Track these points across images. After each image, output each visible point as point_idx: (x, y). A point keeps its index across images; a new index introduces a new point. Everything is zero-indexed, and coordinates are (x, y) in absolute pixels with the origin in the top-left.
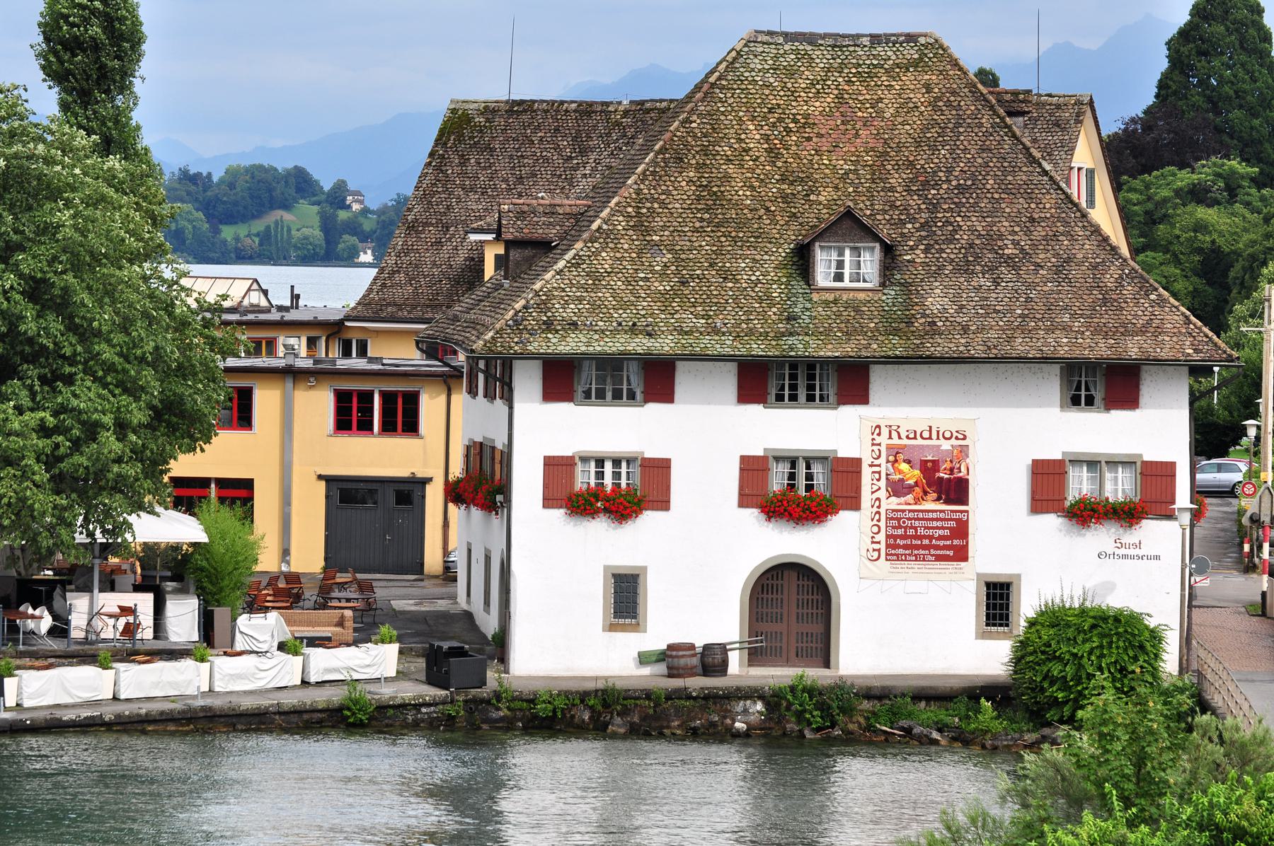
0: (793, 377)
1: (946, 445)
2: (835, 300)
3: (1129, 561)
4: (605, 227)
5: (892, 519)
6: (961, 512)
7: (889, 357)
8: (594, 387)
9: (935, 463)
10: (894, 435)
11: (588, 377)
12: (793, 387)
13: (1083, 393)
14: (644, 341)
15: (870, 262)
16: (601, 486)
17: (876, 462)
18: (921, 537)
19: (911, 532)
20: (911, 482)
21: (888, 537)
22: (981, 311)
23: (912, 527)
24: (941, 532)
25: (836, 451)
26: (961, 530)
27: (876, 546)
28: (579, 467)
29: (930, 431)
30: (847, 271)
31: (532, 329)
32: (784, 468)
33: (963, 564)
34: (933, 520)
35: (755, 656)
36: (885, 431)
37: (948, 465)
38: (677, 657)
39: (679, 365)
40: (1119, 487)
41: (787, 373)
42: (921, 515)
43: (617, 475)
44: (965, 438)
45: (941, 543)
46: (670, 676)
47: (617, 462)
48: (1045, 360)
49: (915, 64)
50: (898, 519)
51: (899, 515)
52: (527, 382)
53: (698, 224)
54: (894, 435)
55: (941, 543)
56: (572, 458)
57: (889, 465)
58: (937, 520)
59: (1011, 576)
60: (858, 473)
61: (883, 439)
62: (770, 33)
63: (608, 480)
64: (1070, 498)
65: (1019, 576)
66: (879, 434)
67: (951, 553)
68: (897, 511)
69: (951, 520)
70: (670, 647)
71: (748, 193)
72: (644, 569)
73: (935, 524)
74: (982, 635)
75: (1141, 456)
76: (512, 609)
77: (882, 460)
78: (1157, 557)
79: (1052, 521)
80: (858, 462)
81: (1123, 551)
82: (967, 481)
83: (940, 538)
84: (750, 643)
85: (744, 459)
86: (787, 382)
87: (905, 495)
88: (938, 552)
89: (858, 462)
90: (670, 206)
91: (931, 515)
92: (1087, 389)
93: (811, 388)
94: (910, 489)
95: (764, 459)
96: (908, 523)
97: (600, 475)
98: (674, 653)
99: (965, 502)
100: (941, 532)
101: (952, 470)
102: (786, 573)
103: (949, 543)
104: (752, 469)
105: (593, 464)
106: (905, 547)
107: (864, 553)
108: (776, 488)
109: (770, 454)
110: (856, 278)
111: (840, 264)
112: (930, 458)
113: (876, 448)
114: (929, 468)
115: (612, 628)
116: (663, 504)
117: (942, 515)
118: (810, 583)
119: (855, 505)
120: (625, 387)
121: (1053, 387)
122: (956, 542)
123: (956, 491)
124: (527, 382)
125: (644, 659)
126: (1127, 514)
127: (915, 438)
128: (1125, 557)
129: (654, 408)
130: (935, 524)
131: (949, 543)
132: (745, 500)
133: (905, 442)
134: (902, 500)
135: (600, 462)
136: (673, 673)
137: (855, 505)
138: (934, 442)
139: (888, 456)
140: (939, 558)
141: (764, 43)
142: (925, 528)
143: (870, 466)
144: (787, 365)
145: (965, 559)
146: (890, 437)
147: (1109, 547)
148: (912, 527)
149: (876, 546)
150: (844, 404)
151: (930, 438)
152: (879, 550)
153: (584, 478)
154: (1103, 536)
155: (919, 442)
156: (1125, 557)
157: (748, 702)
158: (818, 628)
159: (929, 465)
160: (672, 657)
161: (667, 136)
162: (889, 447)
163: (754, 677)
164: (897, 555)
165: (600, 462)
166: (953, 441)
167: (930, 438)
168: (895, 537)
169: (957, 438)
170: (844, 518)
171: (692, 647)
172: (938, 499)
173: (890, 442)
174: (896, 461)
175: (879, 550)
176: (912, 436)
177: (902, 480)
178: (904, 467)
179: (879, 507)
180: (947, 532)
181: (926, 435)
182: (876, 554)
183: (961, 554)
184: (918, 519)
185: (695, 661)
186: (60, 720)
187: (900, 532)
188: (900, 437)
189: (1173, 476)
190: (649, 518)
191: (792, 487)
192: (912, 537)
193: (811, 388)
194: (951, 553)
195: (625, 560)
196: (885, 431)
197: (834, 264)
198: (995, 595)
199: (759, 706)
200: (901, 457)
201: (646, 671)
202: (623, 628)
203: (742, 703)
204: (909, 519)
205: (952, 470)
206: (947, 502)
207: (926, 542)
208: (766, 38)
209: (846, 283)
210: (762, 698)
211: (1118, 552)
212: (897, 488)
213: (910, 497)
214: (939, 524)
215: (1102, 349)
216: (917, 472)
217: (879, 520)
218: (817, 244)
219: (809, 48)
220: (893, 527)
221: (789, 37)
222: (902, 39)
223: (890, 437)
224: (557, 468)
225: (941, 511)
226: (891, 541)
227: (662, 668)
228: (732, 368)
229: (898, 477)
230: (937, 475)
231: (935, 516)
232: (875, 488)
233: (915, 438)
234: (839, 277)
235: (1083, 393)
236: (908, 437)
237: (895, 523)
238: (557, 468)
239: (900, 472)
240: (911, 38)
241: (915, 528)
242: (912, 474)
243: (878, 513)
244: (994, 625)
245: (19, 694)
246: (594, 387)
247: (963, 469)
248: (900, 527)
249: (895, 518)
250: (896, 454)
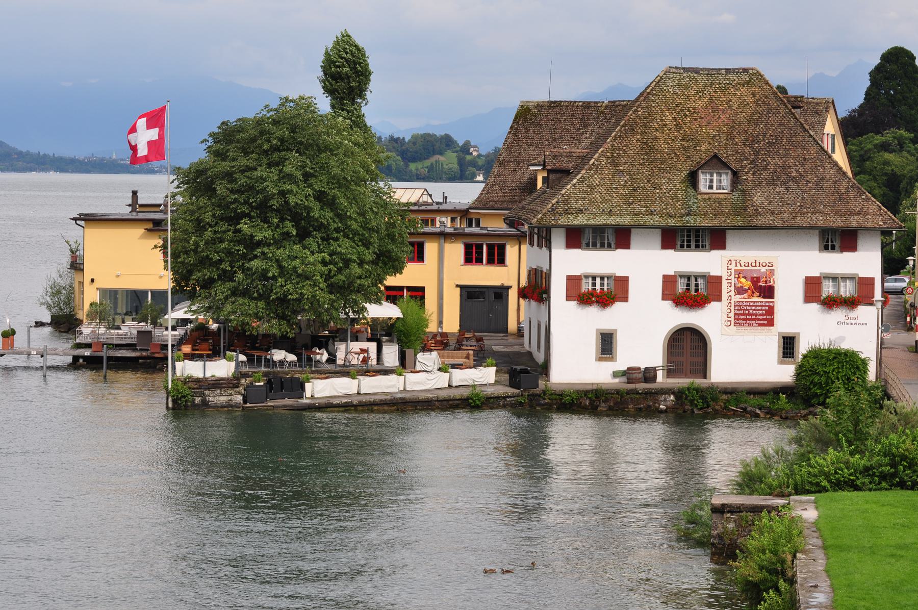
0: (688, 236)
1: (763, 270)
2: (709, 198)
4: (596, 163)
5: (737, 306)
6: (771, 302)
7: (735, 226)
8: (591, 241)
9: (758, 278)
10: (738, 264)
11: (588, 236)
12: (689, 241)
13: (830, 244)
15: (726, 180)
16: (594, 289)
17: (729, 278)
18: (751, 315)
19: (746, 312)
20: (747, 288)
21: (735, 314)
22: (780, 204)
23: (746, 310)
24: (761, 312)
25: (709, 273)
26: (771, 311)
27: (729, 319)
28: (584, 280)
29: (756, 262)
30: (715, 184)
31: (561, 213)
32: (685, 281)
33: (771, 328)
34: (757, 306)
35: (670, 373)
36: (733, 263)
37: (764, 279)
38: (632, 373)
39: (633, 230)
40: (847, 290)
42: (751, 304)
43: (602, 285)
44: (772, 266)
45: (761, 317)
46: (628, 383)
47: (602, 278)
48: (811, 228)
49: (748, 83)
50: (740, 306)
51: (740, 304)
52: (559, 239)
53: (641, 161)
54: (738, 264)
55: (761, 317)
56: (580, 276)
57: (736, 279)
58: (759, 306)
59: (795, 333)
60: (721, 283)
61: (733, 267)
62: (677, 68)
63: (598, 287)
64: (824, 295)
65: (799, 333)
66: (731, 264)
67: (766, 322)
68: (740, 302)
69: (766, 306)
70: (629, 369)
71: (666, 146)
72: (616, 330)
73: (758, 308)
74: (781, 362)
75: (858, 274)
76: (551, 350)
77: (732, 277)
78: (865, 324)
79: (815, 307)
80: (720, 278)
82: (774, 287)
83: (761, 315)
84: (667, 366)
85: (664, 276)
86: (685, 239)
87: (743, 294)
88: (761, 322)
89: (720, 278)
90: (628, 153)
91: (756, 304)
92: (832, 242)
93: (697, 241)
94: (746, 291)
95: (674, 276)
96: (745, 308)
97: (594, 284)
98: (630, 372)
99: (773, 297)
100: (761, 312)
101: (766, 282)
103: (765, 317)
104: (669, 282)
105: (590, 279)
106: (743, 319)
107: (723, 322)
108: (680, 291)
109: (677, 274)
110: (719, 187)
111: (711, 181)
112: (755, 276)
113: (729, 271)
114: (755, 281)
115: (600, 359)
116: (625, 299)
117: (761, 304)
118: (697, 337)
119: (719, 299)
120: (606, 241)
121: (815, 241)
122: (768, 317)
123: (768, 292)
124: (559, 239)
125: (615, 374)
126: (851, 303)
127: (748, 266)
128: (850, 324)
129: (621, 252)
130: (758, 308)
131: (765, 317)
132: (665, 297)
133: (743, 268)
134: (742, 296)
135: (594, 278)
136: (630, 381)
137: (719, 299)
138: (757, 268)
139: (735, 275)
140: (760, 325)
141: (674, 73)
142: (753, 310)
143: (727, 280)
144: (686, 231)
145: (773, 325)
146: (736, 266)
147: (843, 319)
148: (746, 310)
149: (729, 319)
150: (714, 249)
151: (756, 266)
152: (731, 321)
153: (586, 286)
154: (839, 314)
155: (750, 268)
156: (850, 324)
157: (667, 395)
158: (701, 359)
159: (755, 279)
160: (629, 374)
161: (627, 118)
162: (735, 271)
163: (668, 383)
164: (740, 323)
165: (594, 278)
166: (767, 268)
167: (756, 266)
168: (739, 315)
169: (769, 266)
170: (713, 306)
171: (639, 368)
172: (760, 296)
173: (736, 268)
174: (739, 277)
175: (731, 321)
176: (747, 265)
177: (742, 287)
178: (743, 280)
179: (731, 300)
180: (764, 312)
181: (754, 264)
182: (729, 323)
183: (771, 323)
184: (750, 306)
185: (641, 376)
186: (332, 404)
187: (741, 312)
188: (741, 266)
190: (618, 305)
191: (688, 290)
192: (746, 315)
193: (697, 241)
194: (766, 322)
195: (607, 326)
196: (733, 263)
197: (708, 181)
198: (787, 342)
199: (672, 397)
200: (741, 275)
201: (617, 380)
202: (606, 360)
204: (745, 306)
205: (766, 282)
206: (764, 297)
207: (754, 317)
208: (674, 70)
209: (715, 190)
210: (673, 393)
211: (846, 321)
212: (740, 291)
213: (746, 295)
214: (760, 308)
215: (839, 223)
216: (749, 283)
217: (731, 306)
218: (700, 171)
219: (696, 75)
220: (738, 310)
221: (686, 70)
222: (740, 71)
223: (736, 266)
224: (573, 282)
225: (761, 302)
226: (737, 317)
227: (624, 379)
228: (659, 232)
229: (740, 285)
230: (759, 284)
231: (758, 304)
232: (729, 290)
233: (748, 266)
234: (711, 187)
235: (830, 244)
236: (745, 266)
237: (738, 308)
238: (573, 282)
239: (741, 283)
240: (745, 70)
241: (748, 310)
242: (747, 284)
243: (730, 303)
244: (787, 357)
245: (313, 391)
246: (591, 241)
247: (772, 281)
248: (741, 310)
249: (738, 305)
250: (739, 274)
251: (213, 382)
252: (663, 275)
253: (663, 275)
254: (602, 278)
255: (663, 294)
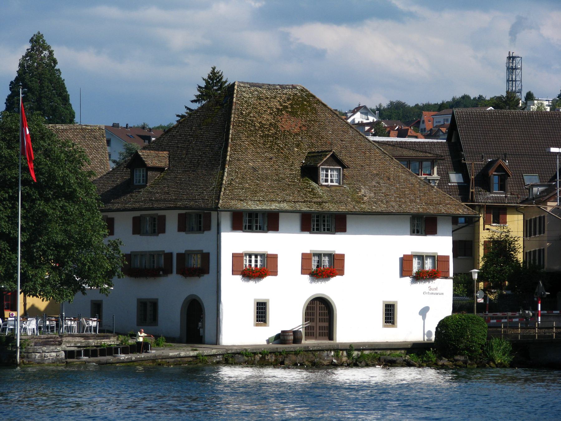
0: (317, 221)
3: (433, 295)
7: (369, 212)
12: (317, 225)
14: (277, 205)
25: (335, 251)
30: (329, 178)
32: (316, 258)
39: (280, 214)
41: (315, 219)
47: (256, 256)
52: (226, 222)
56: (242, 254)
59: (394, 302)
75: (437, 253)
76: (221, 317)
78: (442, 294)
79: (408, 279)
81: (431, 292)
85: (303, 254)
86: (315, 223)
93: (324, 225)
97: (250, 261)
102: (315, 302)
104: (306, 258)
105: (248, 257)
109: (312, 252)
110: (332, 181)
111: (327, 175)
115: (257, 325)
116: (275, 273)
118: (324, 306)
126: (432, 276)
128: (432, 293)
132: (303, 272)
150: (338, 232)
156: (432, 293)
158: (326, 324)
161: (232, 123)
163: (307, 344)
165: (250, 256)
189: (448, 261)
195: (262, 297)
199: (333, 353)
202: (261, 325)
203: (326, 352)
215: (431, 210)
221: (252, 85)
224: (237, 258)
234: (326, 181)
238: (237, 258)
240: (294, 87)
251: (44, 340)
252: (277, 255)
253: (277, 255)
254: (256, 256)
255: (302, 269)
